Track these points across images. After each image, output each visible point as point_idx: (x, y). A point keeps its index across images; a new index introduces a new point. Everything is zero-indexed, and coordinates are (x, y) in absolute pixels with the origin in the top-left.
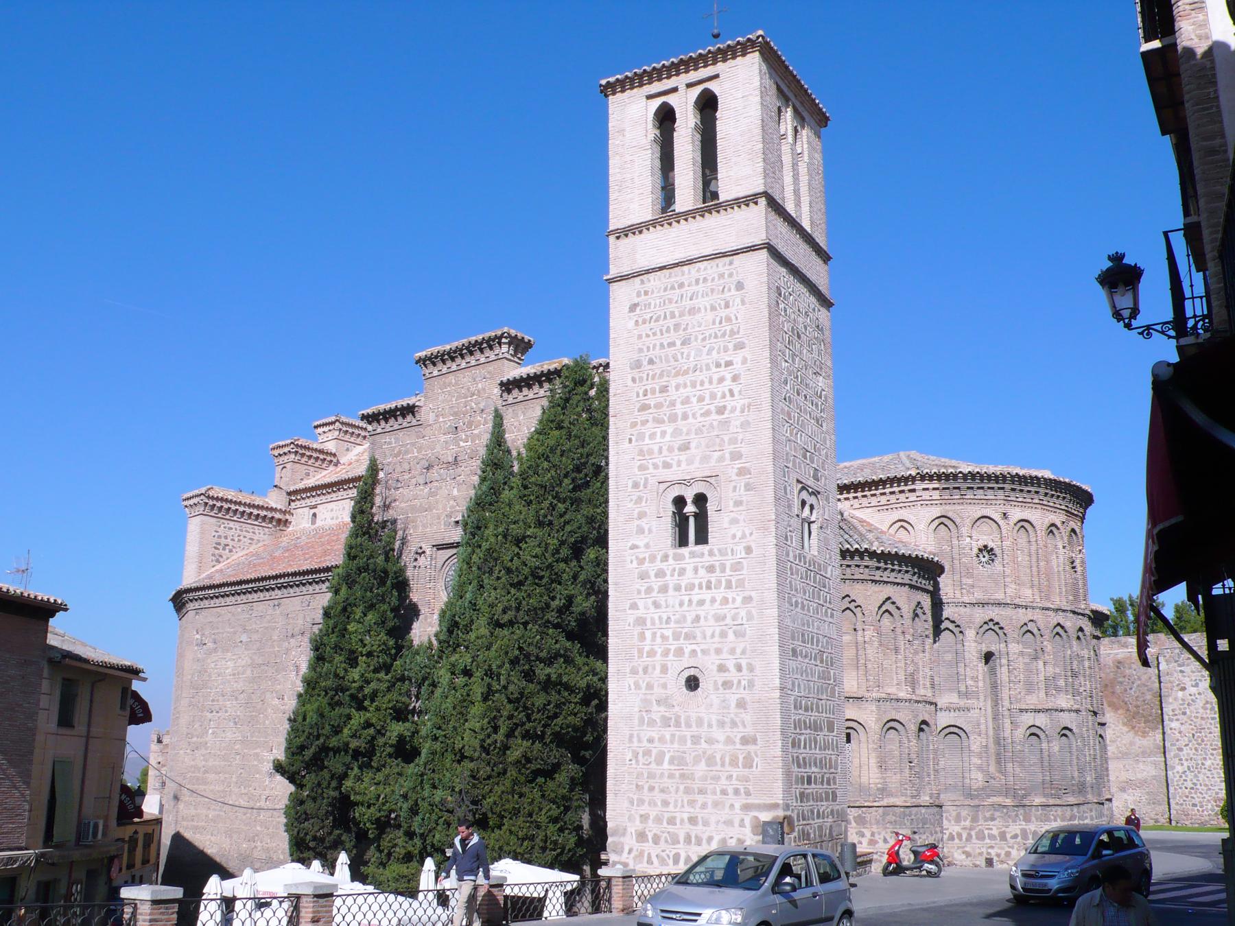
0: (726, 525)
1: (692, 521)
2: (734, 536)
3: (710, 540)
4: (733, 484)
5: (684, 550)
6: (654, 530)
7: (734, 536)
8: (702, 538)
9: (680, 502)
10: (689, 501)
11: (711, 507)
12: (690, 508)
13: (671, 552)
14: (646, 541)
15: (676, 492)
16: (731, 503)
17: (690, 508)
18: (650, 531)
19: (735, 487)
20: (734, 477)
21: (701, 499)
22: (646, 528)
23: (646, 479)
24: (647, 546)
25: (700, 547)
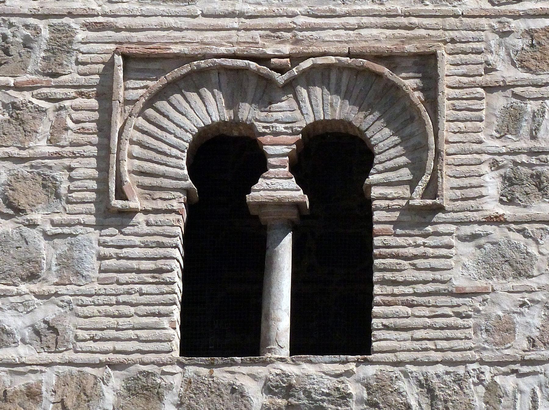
0: (460, 281)
1: (284, 252)
2: (505, 329)
3: (381, 340)
4: (500, 101)
5: (245, 377)
6: (91, 265)
7: (505, 329)
8: (337, 319)
9: (223, 160)
10: (278, 150)
11: (387, 187)
12: (278, 186)
13: (177, 378)
14: (47, 312)
15: (207, 109)
16: (492, 184)
17: (278, 186)
18: (69, 266)
19: (511, 122)
20: (507, 72)
21: (333, 160)
22: (48, 253)
23: (62, 44)
24: (48, 334)
25: (317, 372)
